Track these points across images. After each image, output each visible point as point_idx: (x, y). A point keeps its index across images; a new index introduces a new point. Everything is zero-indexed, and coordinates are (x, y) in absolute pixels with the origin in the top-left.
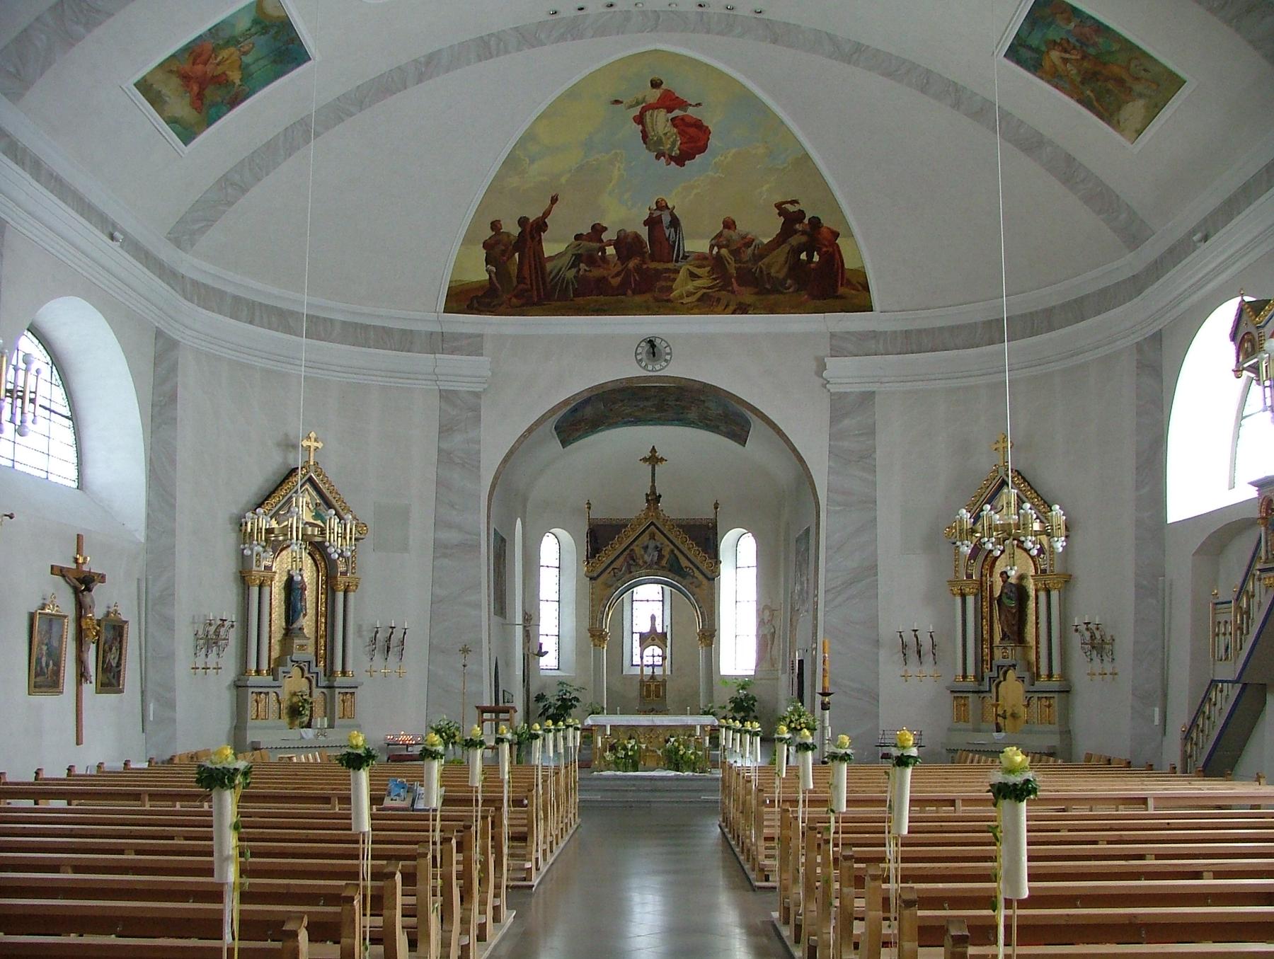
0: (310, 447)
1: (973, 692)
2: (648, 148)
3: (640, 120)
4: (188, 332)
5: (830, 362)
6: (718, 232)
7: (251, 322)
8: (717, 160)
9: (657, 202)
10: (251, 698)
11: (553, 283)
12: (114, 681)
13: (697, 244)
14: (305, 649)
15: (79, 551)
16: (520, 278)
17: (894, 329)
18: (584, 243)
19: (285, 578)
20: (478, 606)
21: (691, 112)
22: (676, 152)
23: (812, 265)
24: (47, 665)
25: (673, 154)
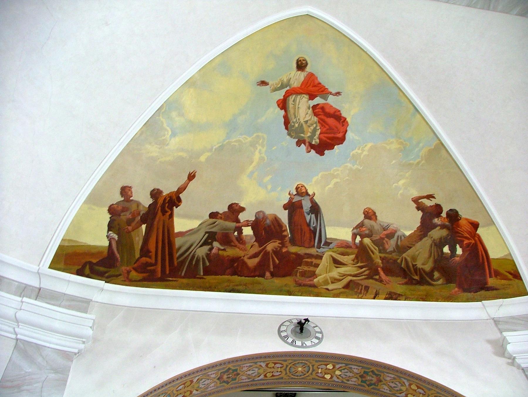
2: (289, 134)
3: (283, 104)
8: (354, 152)
9: (297, 188)
16: (145, 251)
18: (219, 221)
21: (331, 100)
22: (316, 141)
23: (457, 259)
25: (313, 143)
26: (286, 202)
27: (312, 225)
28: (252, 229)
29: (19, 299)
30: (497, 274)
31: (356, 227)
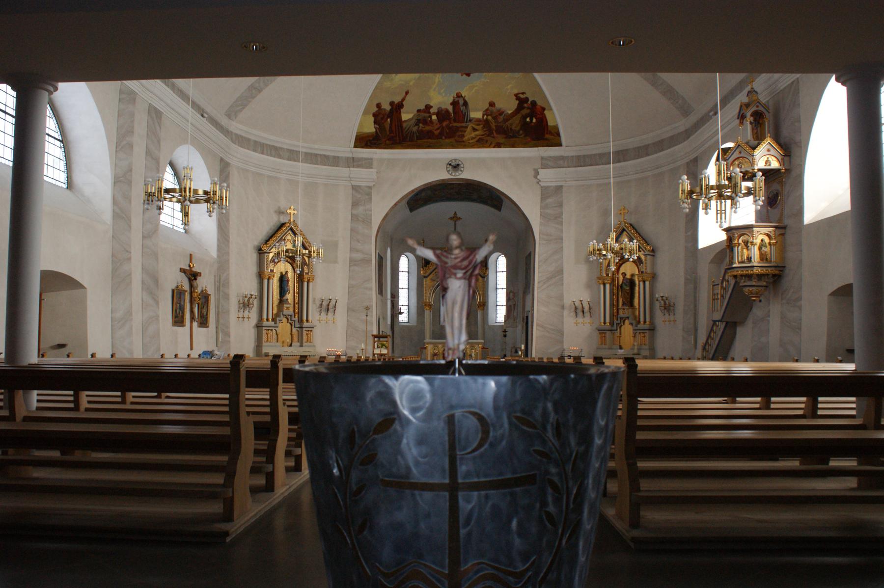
0: (291, 213)
1: (609, 330)
4: (234, 158)
5: (541, 171)
6: (486, 108)
7: (262, 153)
9: (457, 94)
10: (264, 332)
11: (406, 133)
12: (205, 322)
13: (476, 114)
14: (289, 310)
15: (191, 261)
16: (391, 131)
17: (572, 155)
19: (279, 276)
20: (371, 289)
24: (179, 313)
26: (451, 100)
27: (464, 112)
28: (437, 116)
29: (348, 169)
30: (551, 133)
31: (485, 111)
